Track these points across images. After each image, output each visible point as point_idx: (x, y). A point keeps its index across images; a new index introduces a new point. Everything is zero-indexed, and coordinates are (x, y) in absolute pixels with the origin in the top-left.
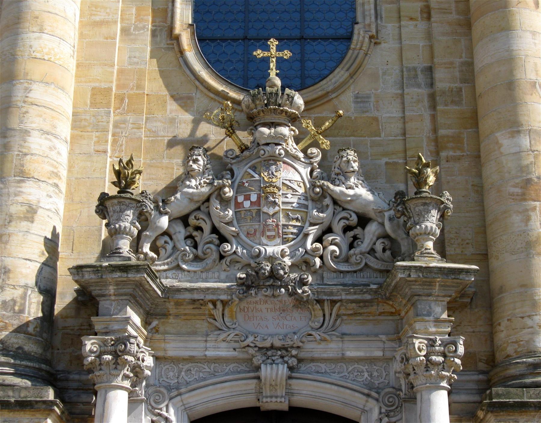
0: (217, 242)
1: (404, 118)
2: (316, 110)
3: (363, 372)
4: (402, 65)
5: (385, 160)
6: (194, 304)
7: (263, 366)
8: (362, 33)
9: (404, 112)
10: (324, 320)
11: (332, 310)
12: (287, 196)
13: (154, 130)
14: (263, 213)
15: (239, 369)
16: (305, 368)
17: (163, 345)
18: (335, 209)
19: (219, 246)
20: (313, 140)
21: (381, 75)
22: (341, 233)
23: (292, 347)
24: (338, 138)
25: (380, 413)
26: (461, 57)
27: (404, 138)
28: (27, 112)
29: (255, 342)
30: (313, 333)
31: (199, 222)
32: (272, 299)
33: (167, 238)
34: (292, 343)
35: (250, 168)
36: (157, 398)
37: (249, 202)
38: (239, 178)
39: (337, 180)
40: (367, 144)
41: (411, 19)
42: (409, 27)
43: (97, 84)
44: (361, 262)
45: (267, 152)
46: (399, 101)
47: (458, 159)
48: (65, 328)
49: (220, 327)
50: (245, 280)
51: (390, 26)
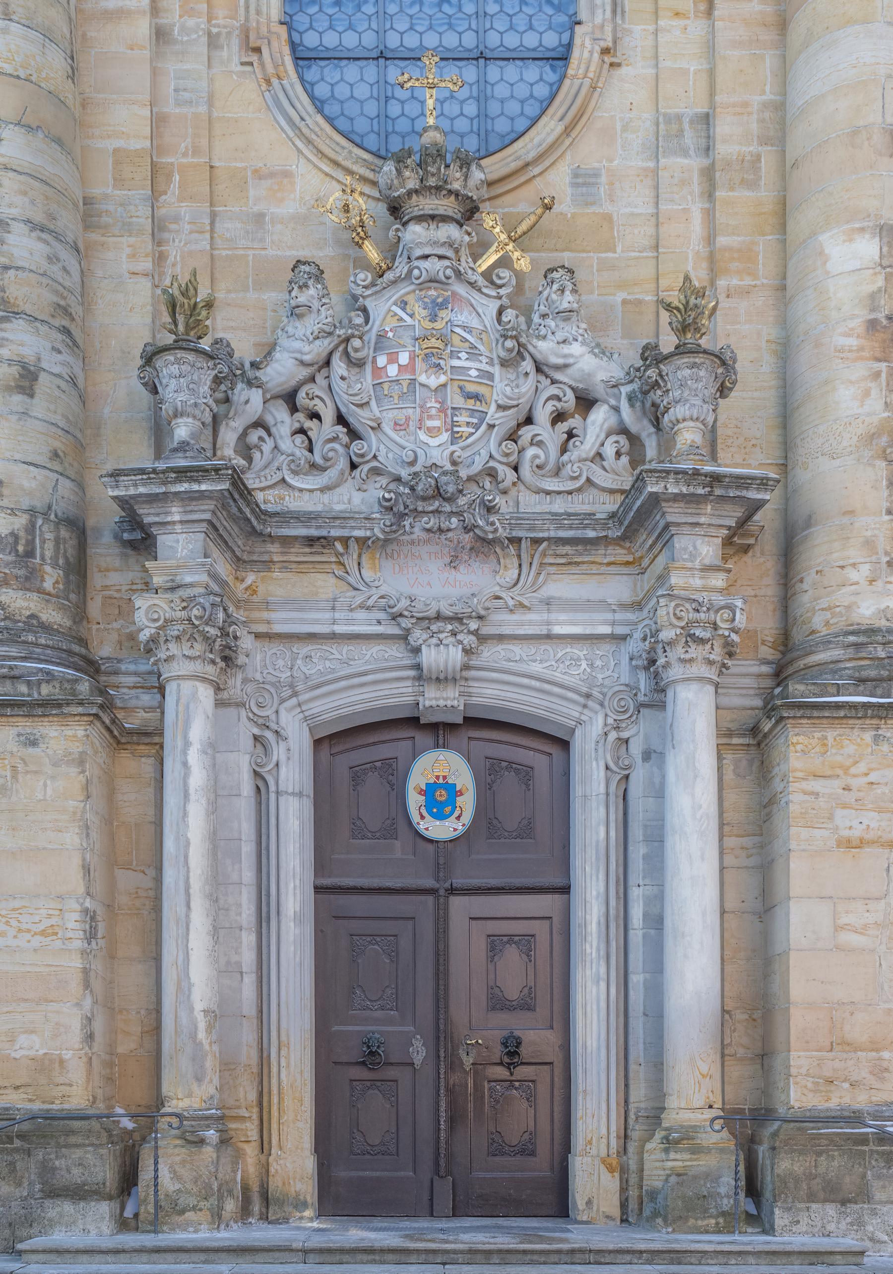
0: (345, 439)
2: (507, 199)
3: (579, 659)
4: (657, 111)
6: (312, 545)
7: (423, 647)
10: (519, 575)
11: (532, 557)
12: (460, 355)
13: (228, 236)
14: (421, 385)
15: (386, 655)
16: (489, 654)
17: (265, 615)
18: (538, 382)
20: (502, 253)
21: (619, 132)
22: (549, 425)
23: (470, 617)
24: (543, 254)
25: (606, 725)
27: (655, 254)
29: (411, 609)
30: (503, 595)
33: (261, 432)
34: (470, 610)
35: (395, 304)
37: (395, 366)
38: (377, 323)
39: (542, 327)
40: (592, 266)
44: (580, 475)
45: (424, 273)
47: (746, 292)
48: (106, 587)
50: (393, 501)
51: (637, 29)
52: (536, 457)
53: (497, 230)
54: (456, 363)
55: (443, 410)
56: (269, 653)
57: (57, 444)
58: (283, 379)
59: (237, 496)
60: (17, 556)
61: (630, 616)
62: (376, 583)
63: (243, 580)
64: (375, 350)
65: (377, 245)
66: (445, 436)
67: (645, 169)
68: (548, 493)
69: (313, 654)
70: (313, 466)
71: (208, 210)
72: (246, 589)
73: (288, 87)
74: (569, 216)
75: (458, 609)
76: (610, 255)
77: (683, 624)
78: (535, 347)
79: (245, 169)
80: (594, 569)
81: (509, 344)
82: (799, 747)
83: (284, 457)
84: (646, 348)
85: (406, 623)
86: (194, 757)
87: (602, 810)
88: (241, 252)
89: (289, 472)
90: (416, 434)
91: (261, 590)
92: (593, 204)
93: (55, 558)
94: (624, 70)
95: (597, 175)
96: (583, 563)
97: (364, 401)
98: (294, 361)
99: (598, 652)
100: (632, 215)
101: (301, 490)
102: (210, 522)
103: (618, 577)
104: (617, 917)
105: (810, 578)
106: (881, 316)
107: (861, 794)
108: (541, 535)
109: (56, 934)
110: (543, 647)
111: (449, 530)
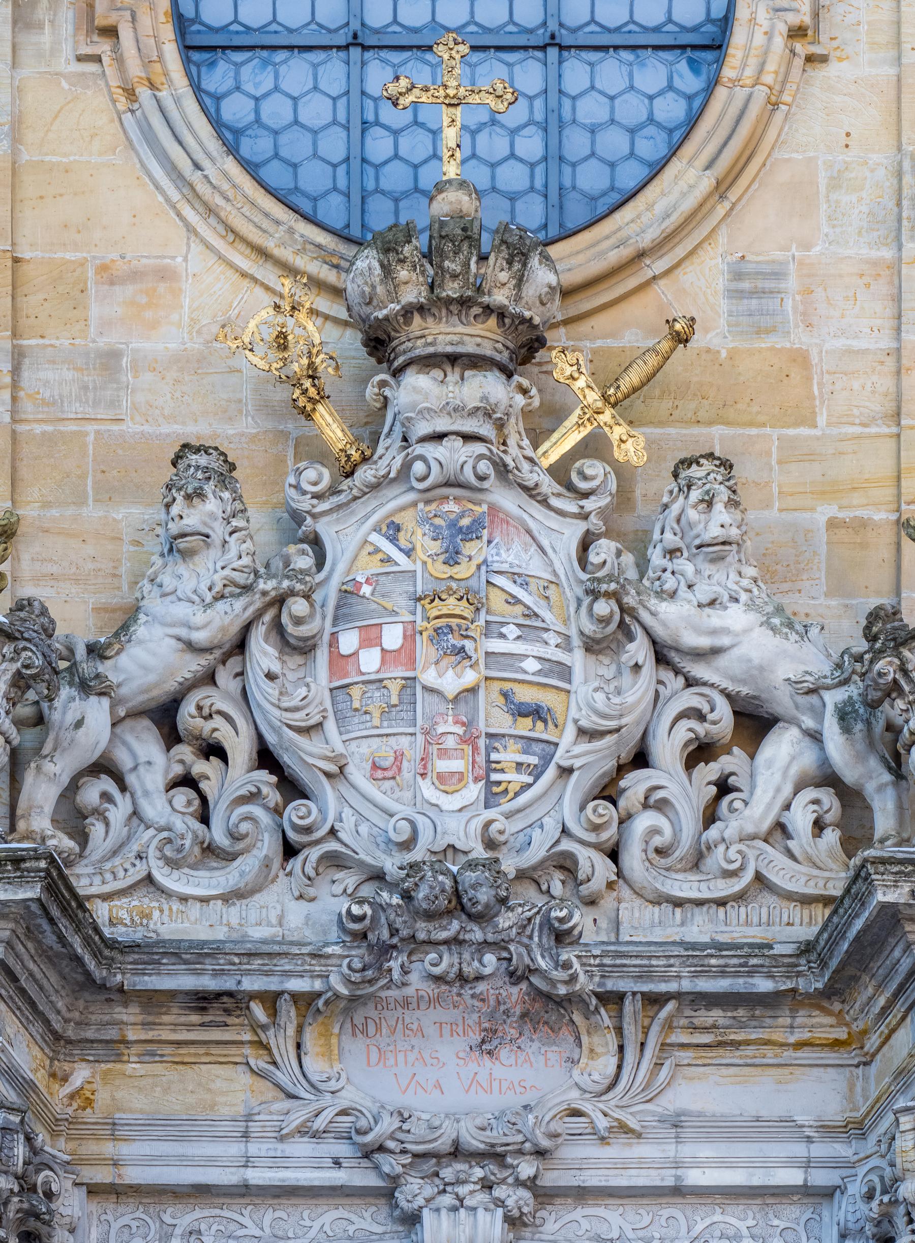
0: (274, 797)
2: (600, 322)
4: (899, 149)
6: (204, 1009)
7: (426, 1213)
10: (620, 1067)
11: (646, 1031)
12: (504, 630)
13: (47, 395)
14: (427, 689)
15: (351, 1229)
16: (557, 1226)
17: (108, 1149)
18: (660, 682)
20: (589, 428)
21: (823, 189)
22: (680, 768)
23: (520, 1152)
24: (672, 431)
27: (894, 430)
30: (586, 1107)
31: (210, 725)
33: (106, 784)
34: (520, 1138)
35: (376, 529)
37: (376, 653)
38: (341, 567)
39: (668, 574)
40: (769, 454)
44: (742, 868)
45: (435, 467)
46: (882, 288)
49: (290, 1088)
50: (367, 922)
52: (655, 831)
53: (581, 383)
54: (496, 645)
55: (469, 739)
56: (116, 1226)
58: (152, 678)
59: (55, 912)
61: (841, 1150)
62: (333, 1085)
63: (65, 1079)
64: (336, 620)
65: (341, 413)
66: (474, 791)
67: (875, 263)
68: (678, 903)
69: (203, 1227)
70: (209, 850)
71: (8, 345)
72: (72, 1096)
73: (169, 104)
74: (724, 354)
75: (495, 1136)
76: (804, 431)
78: (653, 614)
79: (82, 263)
80: (770, 1055)
81: (603, 607)
83: (151, 832)
84: (874, 616)
85: (390, 1164)
88: (72, 427)
89: (161, 863)
90: (415, 787)
91: (102, 1097)
92: (770, 330)
94: (832, 70)
95: (778, 275)
96: (748, 1043)
97: (312, 722)
98: (173, 642)
99: (776, 1222)
100: (849, 352)
101: (184, 899)
103: (815, 1071)
108: (663, 987)
110: (666, 1213)
111: (479, 978)
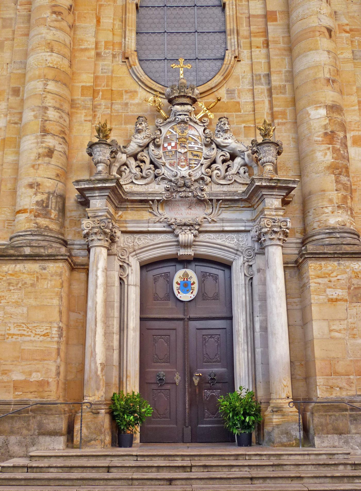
0: (154, 169)
1: (254, 102)
3: (234, 238)
5: (243, 125)
8: (230, 55)
9: (254, 98)
11: (217, 205)
14: (179, 152)
17: (125, 225)
19: (154, 171)
22: (221, 163)
26: (286, 68)
28: (46, 97)
30: (207, 217)
32: (184, 199)
33: (125, 167)
36: (123, 253)
38: (164, 134)
41: (258, 47)
42: (256, 52)
43: (84, 84)
46: (251, 92)
47: (284, 124)
48: (71, 216)
52: (217, 173)
53: (203, 107)
55: (186, 160)
57: (58, 172)
59: (117, 187)
60: (43, 207)
61: (251, 224)
62: (164, 214)
63: (118, 214)
64: (164, 142)
65: (164, 111)
66: (187, 168)
68: (222, 185)
71: (110, 102)
72: (119, 216)
73: (137, 68)
75: (191, 222)
77: (270, 227)
79: (123, 90)
80: (238, 209)
82: (312, 267)
84: (253, 141)
85: (173, 227)
86: (100, 273)
87: (244, 290)
88: (120, 114)
91: (124, 216)
92: (233, 99)
93: (55, 208)
94: (242, 62)
101: (138, 185)
102: (108, 196)
104: (250, 327)
105: (312, 211)
106: (328, 131)
107: (335, 283)
108: (220, 198)
109: (48, 336)
111: (188, 197)
